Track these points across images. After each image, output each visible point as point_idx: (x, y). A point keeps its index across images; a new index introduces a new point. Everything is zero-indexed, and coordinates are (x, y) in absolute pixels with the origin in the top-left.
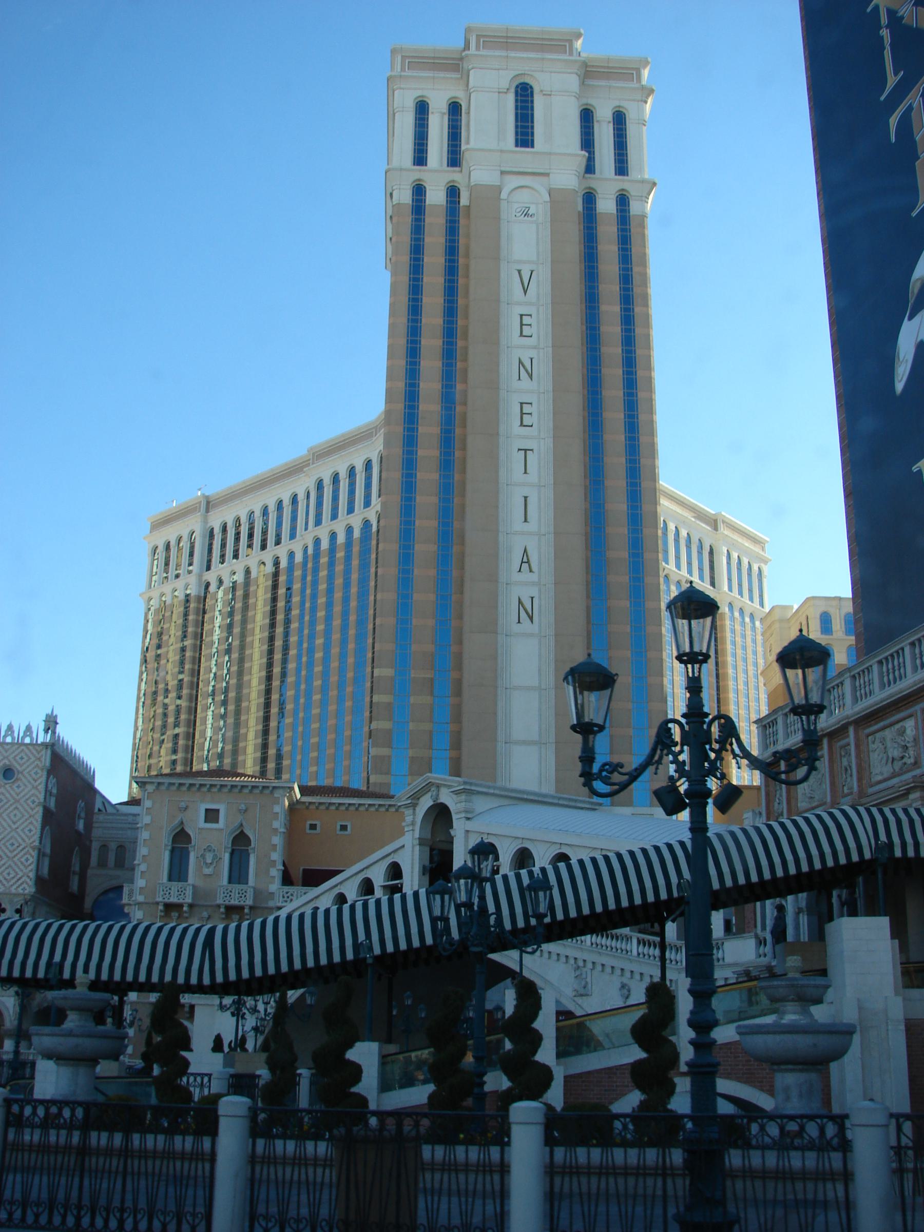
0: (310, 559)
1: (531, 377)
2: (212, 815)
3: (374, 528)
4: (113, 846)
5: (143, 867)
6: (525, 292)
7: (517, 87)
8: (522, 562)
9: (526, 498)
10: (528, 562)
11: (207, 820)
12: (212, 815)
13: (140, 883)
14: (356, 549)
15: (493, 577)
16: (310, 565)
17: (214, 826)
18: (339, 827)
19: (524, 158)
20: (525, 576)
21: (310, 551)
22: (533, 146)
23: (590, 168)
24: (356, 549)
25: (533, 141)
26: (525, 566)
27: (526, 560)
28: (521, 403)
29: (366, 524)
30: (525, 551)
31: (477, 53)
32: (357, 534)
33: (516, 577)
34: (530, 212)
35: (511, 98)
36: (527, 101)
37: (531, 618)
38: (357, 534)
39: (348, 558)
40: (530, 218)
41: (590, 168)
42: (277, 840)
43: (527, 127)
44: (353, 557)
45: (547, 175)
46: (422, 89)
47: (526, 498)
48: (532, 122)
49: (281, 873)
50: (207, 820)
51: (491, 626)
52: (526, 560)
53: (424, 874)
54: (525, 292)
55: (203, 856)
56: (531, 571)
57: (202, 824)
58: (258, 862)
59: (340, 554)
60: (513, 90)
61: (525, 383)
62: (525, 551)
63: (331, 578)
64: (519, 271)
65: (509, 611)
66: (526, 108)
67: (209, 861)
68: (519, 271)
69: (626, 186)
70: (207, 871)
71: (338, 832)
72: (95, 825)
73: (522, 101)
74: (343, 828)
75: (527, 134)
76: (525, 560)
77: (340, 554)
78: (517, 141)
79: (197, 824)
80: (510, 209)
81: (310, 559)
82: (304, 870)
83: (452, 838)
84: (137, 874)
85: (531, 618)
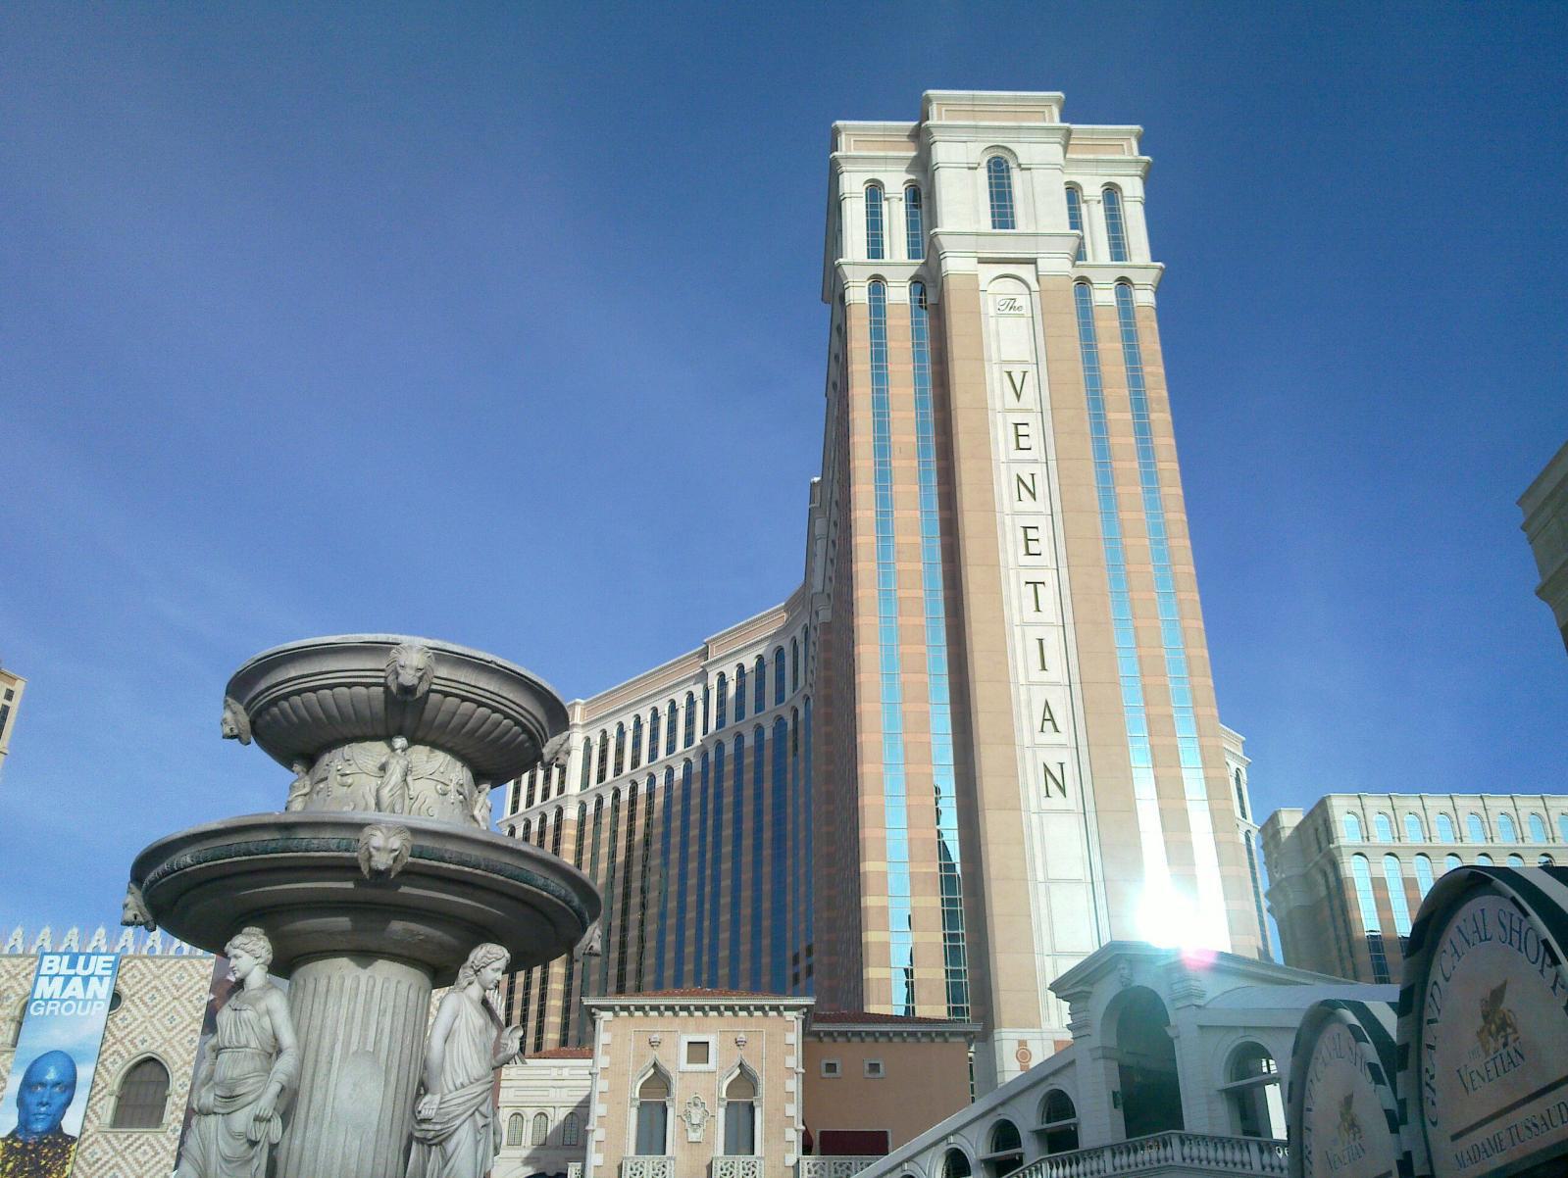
0: (712, 768)
1: (1033, 495)
2: (699, 1051)
4: (530, 1113)
6: (1018, 397)
7: (989, 161)
8: (1044, 720)
9: (1041, 641)
10: (1052, 719)
12: (699, 1051)
14: (768, 753)
15: (1009, 740)
16: (711, 775)
18: (867, 1068)
19: (1007, 246)
20: (1050, 737)
22: (1013, 228)
23: (1079, 255)
24: (768, 753)
25: (1013, 222)
26: (1048, 724)
27: (1048, 717)
28: (1025, 528)
30: (1047, 703)
31: (939, 123)
32: (768, 734)
33: (1041, 739)
34: (1017, 304)
35: (983, 175)
36: (1003, 178)
37: (1063, 790)
38: (768, 734)
39: (759, 764)
40: (1017, 312)
41: (1079, 255)
42: (794, 1085)
43: (1005, 206)
44: (765, 763)
45: (1033, 262)
46: (873, 171)
47: (1041, 641)
48: (1011, 200)
49: (801, 1134)
51: (1013, 804)
52: (1048, 717)
53: (1115, 1107)
54: (1018, 397)
55: (688, 1114)
56: (1057, 731)
58: (767, 1122)
59: (749, 760)
60: (984, 164)
61: (1027, 503)
62: (1047, 703)
63: (738, 788)
64: (1009, 374)
65: (1031, 782)
66: (1002, 185)
68: (1009, 374)
69: (1126, 273)
70: (693, 1136)
71: (867, 1075)
72: (503, 1084)
73: (996, 178)
74: (874, 1067)
75: (1005, 215)
76: (1047, 716)
77: (749, 760)
78: (994, 222)
79: (678, 1062)
80: (989, 306)
81: (712, 768)
82: (823, 1134)
83: (1171, 1041)
84: (592, 1146)
85: (1063, 790)
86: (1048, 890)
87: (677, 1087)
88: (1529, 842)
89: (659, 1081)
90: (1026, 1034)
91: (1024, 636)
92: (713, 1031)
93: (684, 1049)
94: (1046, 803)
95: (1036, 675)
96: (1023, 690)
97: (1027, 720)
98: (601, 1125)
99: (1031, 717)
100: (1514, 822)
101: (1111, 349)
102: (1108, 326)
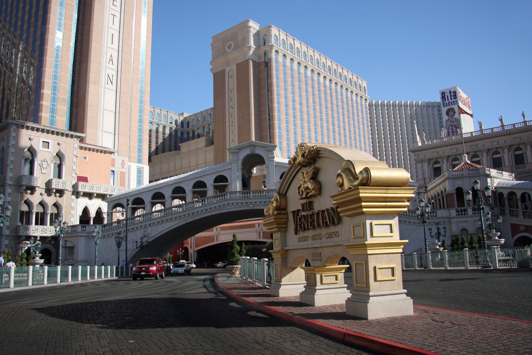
5: (11, 166)
11: (43, 147)
13: (10, 174)
15: (99, 63)
17: (47, 150)
33: (108, 65)
50: (43, 147)
57: (41, 148)
65: (104, 78)
67: (44, 166)
70: (44, 171)
74: (85, 158)
84: (9, 170)
86: (103, 112)
88: (162, 122)
91: (108, 31)
93: (41, 143)
94: (107, 86)
95: (110, 44)
96: (105, 48)
97: (105, 60)
98: (12, 164)
99: (106, 58)
100: (159, 115)
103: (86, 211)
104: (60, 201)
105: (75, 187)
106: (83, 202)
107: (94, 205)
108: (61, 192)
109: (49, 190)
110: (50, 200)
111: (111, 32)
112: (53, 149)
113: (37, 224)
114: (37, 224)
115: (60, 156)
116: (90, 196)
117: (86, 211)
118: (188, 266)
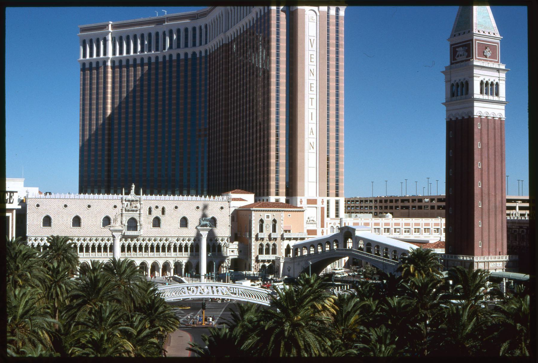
2: (268, 217)
3: (198, 56)
12: (268, 217)
15: (303, 137)
20: (312, 136)
21: (167, 58)
29: (194, 54)
32: (190, 56)
38: (190, 56)
39: (186, 65)
51: (303, 151)
57: (266, 219)
79: (265, 219)
87: (265, 222)
89: (262, 221)
90: (302, 198)
92: (270, 214)
94: (310, 151)
95: (310, 121)
101: (333, 28)
102: (333, 21)
103: (288, 246)
104: (275, 242)
105: (282, 235)
106: (286, 243)
107: (292, 243)
108: (275, 239)
109: (270, 239)
110: (271, 243)
111: (310, 111)
112: (271, 219)
113: (266, 254)
114: (266, 254)
115: (275, 221)
116: (289, 239)
117: (288, 246)
118: (318, 278)
